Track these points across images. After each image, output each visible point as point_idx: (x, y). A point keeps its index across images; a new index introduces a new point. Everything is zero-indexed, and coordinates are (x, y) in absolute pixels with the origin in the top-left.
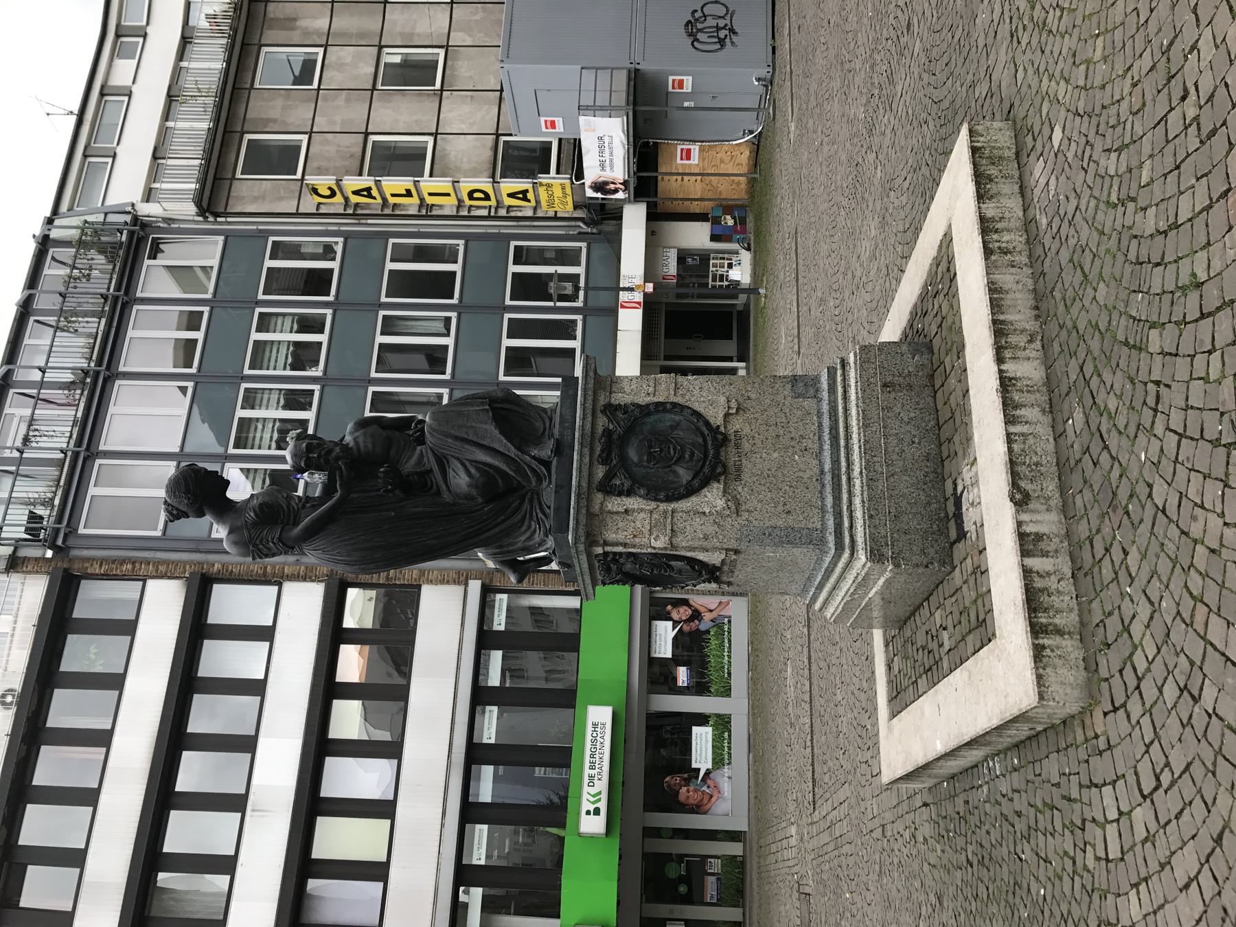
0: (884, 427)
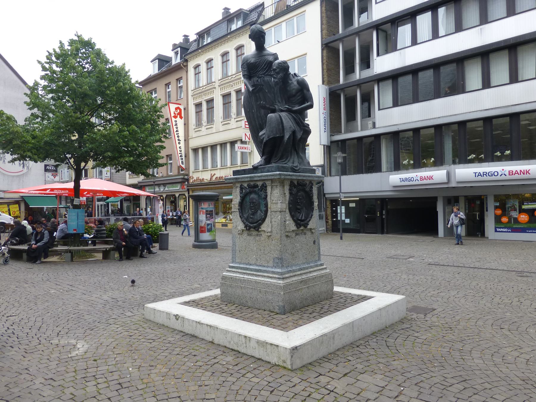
0: (254, 289)
